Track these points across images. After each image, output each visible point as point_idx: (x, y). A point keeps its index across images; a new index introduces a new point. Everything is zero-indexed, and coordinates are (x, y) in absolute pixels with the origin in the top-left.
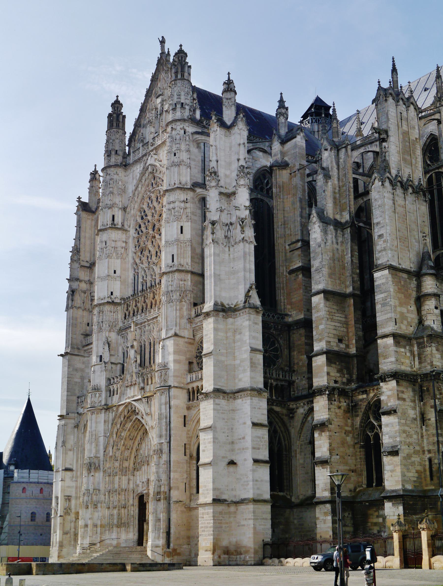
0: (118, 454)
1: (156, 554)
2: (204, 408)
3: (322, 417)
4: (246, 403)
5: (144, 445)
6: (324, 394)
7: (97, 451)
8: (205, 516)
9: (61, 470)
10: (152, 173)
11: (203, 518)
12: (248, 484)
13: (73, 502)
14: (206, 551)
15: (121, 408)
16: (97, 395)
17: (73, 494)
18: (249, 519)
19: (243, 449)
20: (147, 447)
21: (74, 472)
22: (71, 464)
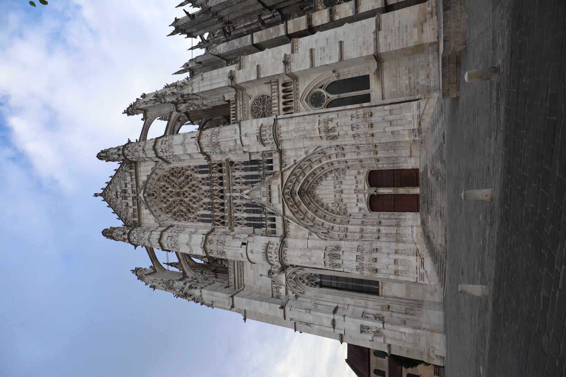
0: (327, 224)
1: (427, 107)
2: (297, 65)
3: (326, 15)
4: (302, 42)
5: (325, 201)
6: (311, 17)
7: (320, 249)
8: (388, 42)
9: (332, 316)
10: (149, 195)
11: (390, 44)
12: (364, 25)
13: (369, 311)
14: (422, 31)
15: (288, 213)
16: (271, 246)
17: (361, 310)
18: (394, 16)
19: (336, 35)
20: (327, 196)
21: (339, 306)
22: (331, 308)
